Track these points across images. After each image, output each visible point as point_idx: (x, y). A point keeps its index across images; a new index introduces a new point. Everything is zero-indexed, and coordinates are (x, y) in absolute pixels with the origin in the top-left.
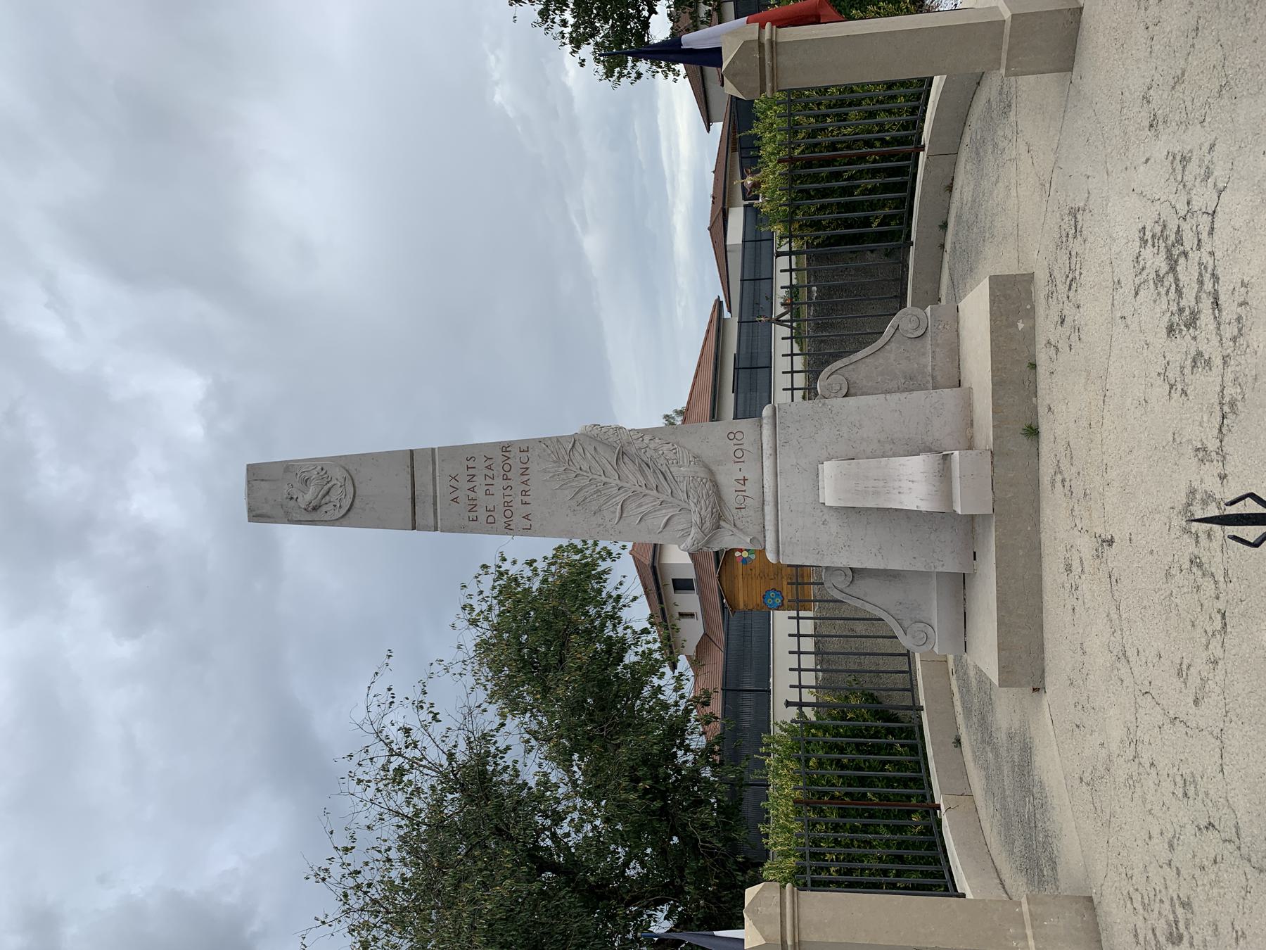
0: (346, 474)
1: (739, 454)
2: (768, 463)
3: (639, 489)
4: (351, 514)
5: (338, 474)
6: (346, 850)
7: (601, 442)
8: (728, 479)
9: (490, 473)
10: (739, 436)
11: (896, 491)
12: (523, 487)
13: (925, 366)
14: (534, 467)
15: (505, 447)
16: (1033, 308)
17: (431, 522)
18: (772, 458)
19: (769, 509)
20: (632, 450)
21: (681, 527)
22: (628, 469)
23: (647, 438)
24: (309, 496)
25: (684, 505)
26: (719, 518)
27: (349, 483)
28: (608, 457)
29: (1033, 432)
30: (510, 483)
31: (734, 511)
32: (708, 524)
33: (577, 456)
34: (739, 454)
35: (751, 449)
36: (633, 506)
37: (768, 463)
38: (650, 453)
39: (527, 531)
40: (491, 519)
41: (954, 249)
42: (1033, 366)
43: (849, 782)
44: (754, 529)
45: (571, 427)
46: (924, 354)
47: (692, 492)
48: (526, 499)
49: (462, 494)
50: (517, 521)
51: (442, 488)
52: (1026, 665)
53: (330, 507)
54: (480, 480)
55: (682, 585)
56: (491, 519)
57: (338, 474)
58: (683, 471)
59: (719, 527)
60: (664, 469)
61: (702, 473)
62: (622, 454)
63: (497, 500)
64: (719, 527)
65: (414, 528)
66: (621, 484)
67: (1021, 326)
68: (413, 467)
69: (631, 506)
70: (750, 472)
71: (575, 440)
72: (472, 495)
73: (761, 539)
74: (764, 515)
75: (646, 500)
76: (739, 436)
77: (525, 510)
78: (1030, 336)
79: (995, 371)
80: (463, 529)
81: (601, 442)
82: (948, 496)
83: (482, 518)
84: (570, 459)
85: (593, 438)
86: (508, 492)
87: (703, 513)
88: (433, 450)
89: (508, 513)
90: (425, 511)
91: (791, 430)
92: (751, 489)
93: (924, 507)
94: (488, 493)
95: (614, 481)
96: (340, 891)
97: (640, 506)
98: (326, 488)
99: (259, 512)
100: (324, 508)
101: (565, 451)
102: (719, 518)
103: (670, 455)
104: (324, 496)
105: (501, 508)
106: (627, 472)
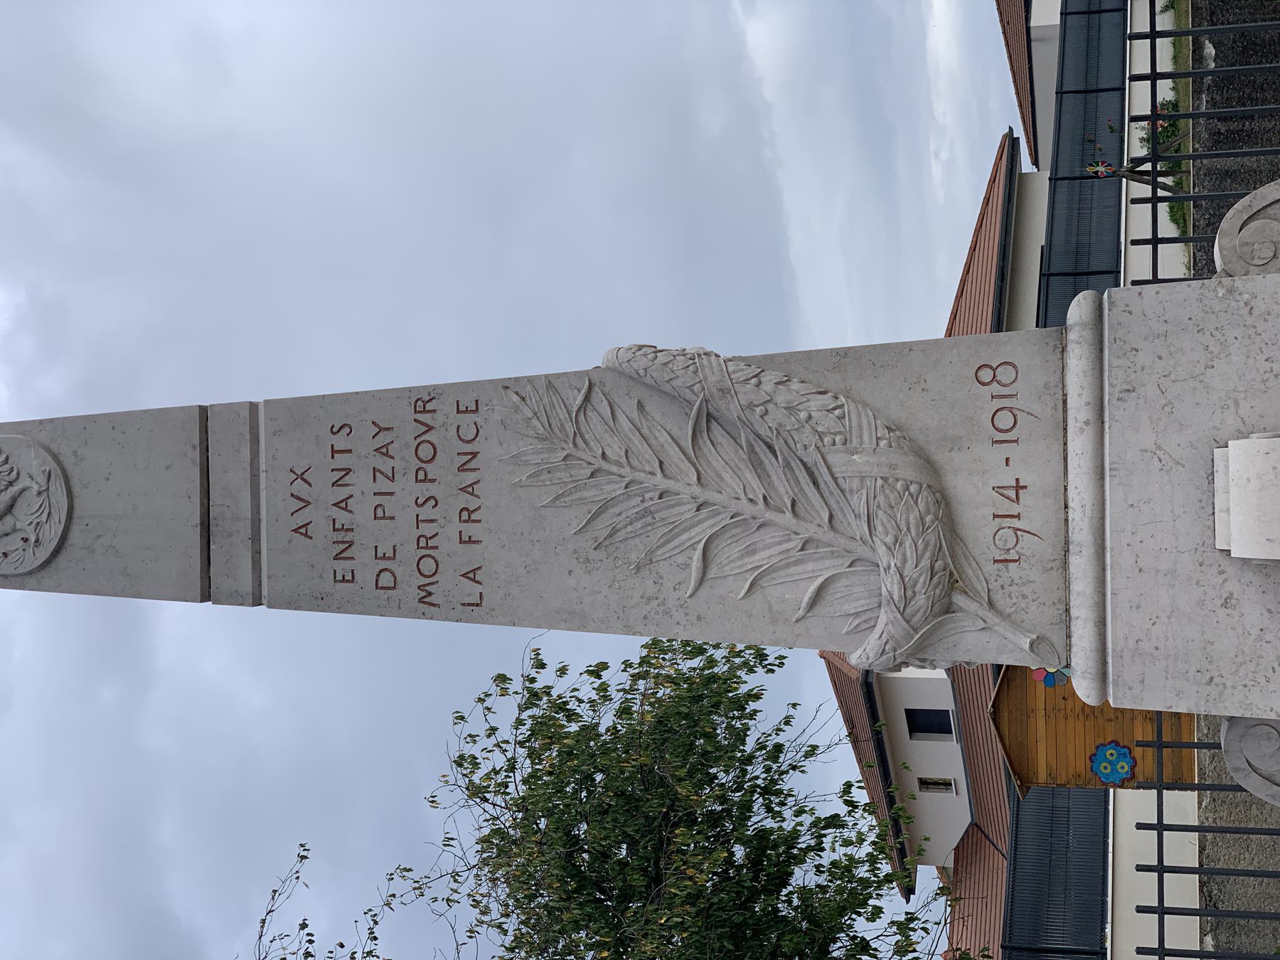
0: (52, 465)
1: (1005, 420)
2: (1079, 444)
4: (62, 559)
5: (32, 464)
7: (656, 389)
8: (975, 485)
9: (386, 465)
10: (1005, 375)
14: (489, 450)
15: (423, 401)
17: (247, 584)
18: (1090, 433)
19: (1080, 565)
20: (731, 409)
21: (850, 607)
22: (723, 457)
23: (769, 379)
25: (862, 551)
26: (948, 585)
27: (58, 489)
28: (671, 427)
30: (432, 489)
31: (990, 568)
32: (921, 601)
33: (595, 424)
34: (1005, 420)
35: (1035, 408)
36: (735, 551)
37: (1079, 444)
38: (777, 415)
39: (473, 609)
40: (386, 579)
44: (1041, 616)
45: (588, 358)
47: (881, 518)
48: (471, 530)
49: (319, 517)
50: (449, 584)
51: (275, 500)
54: (361, 482)
56: (386, 579)
57: (32, 464)
58: (858, 464)
59: (949, 609)
60: (812, 457)
61: (907, 470)
62: (707, 419)
63: (403, 532)
64: (949, 609)
65: (206, 596)
66: (703, 495)
68: (205, 449)
69: (727, 552)
70: (1031, 467)
71: (591, 385)
72: (342, 517)
73: (1058, 640)
75: (767, 536)
76: (1005, 375)
77: (466, 557)
80: (320, 602)
81: (656, 389)
83: (366, 577)
84: (578, 432)
85: (636, 379)
86: (427, 512)
87: (909, 570)
88: (253, 407)
89: (428, 566)
91: (1142, 358)
92: (1035, 512)
94: (379, 514)
95: (686, 485)
97: (750, 551)
101: (566, 410)
102: (948, 585)
105: (410, 552)
106: (718, 464)
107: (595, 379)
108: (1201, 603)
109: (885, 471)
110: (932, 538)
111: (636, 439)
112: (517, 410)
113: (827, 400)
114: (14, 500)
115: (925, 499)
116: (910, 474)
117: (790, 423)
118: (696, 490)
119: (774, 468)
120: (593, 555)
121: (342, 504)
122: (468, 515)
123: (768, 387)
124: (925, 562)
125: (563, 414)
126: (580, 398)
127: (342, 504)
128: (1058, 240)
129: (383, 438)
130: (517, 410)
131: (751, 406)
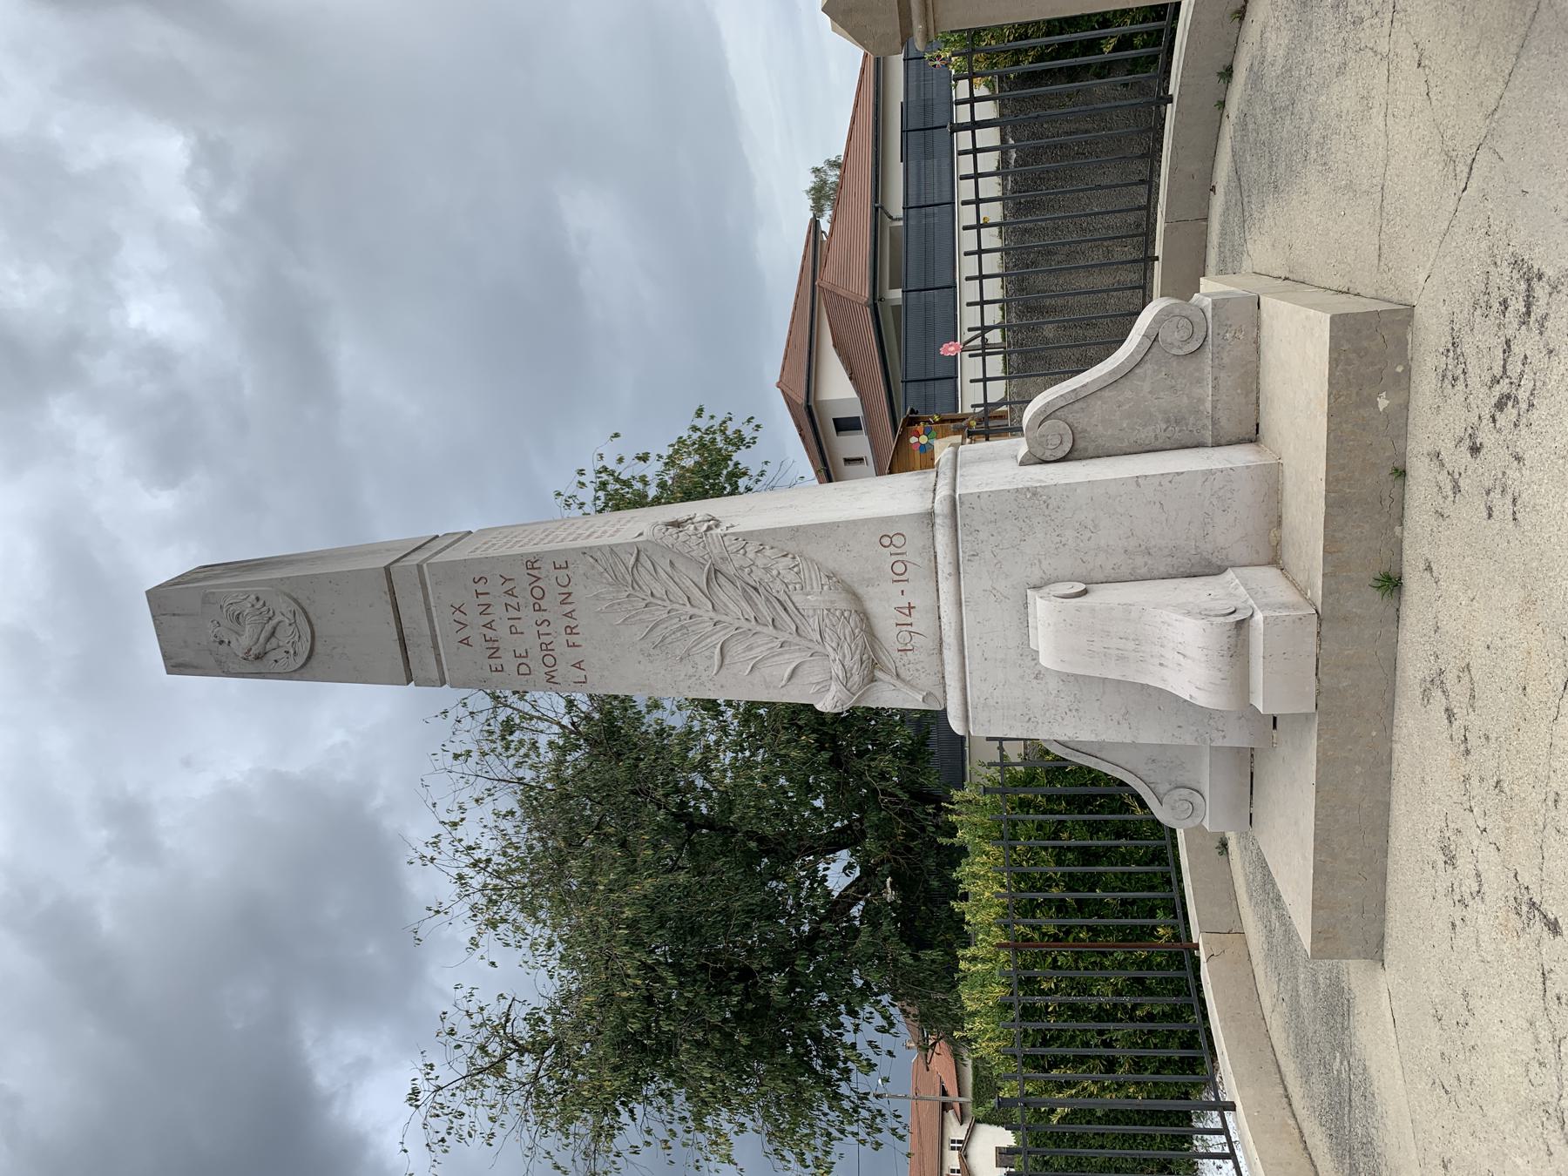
0: (294, 607)
2: (946, 586)
3: (746, 625)
4: (313, 662)
5: (283, 606)
6: (455, 824)
8: (884, 606)
10: (898, 541)
11: (1157, 661)
12: (567, 621)
13: (1201, 401)
14: (580, 591)
16: (1408, 371)
17: (435, 675)
18: (952, 580)
19: (950, 655)
20: (729, 569)
23: (751, 549)
24: (245, 640)
25: (818, 648)
26: (872, 666)
27: (301, 620)
29: (1392, 584)
30: (545, 615)
31: (897, 655)
32: (856, 678)
33: (644, 576)
34: (899, 568)
35: (918, 560)
36: (740, 648)
37: (946, 586)
38: (758, 574)
41: (1243, 124)
42: (1401, 473)
43: (1072, 883)
44: (928, 681)
46: (1199, 381)
47: (828, 633)
52: (1355, 914)
53: (279, 654)
54: (498, 611)
55: (845, 425)
56: (523, 669)
58: (815, 600)
59: (873, 680)
60: (783, 597)
61: (842, 603)
63: (530, 641)
64: (873, 680)
67: (1383, 403)
69: (735, 650)
70: (921, 600)
73: (939, 694)
74: (942, 661)
75: (759, 640)
76: (898, 541)
77: (573, 655)
78: (1398, 423)
79: (1330, 482)
82: (1240, 682)
84: (634, 580)
86: (544, 629)
90: (421, 656)
91: (982, 536)
92: (921, 622)
93: (1202, 700)
94: (513, 631)
96: (454, 872)
97: (749, 648)
98: (269, 627)
99: (180, 660)
100: (272, 656)
102: (872, 666)
103: (790, 577)
104: (268, 640)
105: (536, 653)
106: (725, 599)
107: (641, 547)
108: (1022, 677)
109: (828, 605)
110: (859, 641)
111: (671, 584)
112: (593, 567)
113: (788, 561)
114: (275, 629)
115: (854, 619)
116: (842, 605)
117: (767, 578)
118: (712, 614)
119: (760, 602)
120: (652, 652)
121: (488, 626)
122: (570, 630)
123: (751, 555)
124: (857, 657)
125: (623, 570)
126: (633, 560)
127: (488, 626)
128: (912, 98)
129: (509, 585)
130: (593, 567)
131: (742, 568)
